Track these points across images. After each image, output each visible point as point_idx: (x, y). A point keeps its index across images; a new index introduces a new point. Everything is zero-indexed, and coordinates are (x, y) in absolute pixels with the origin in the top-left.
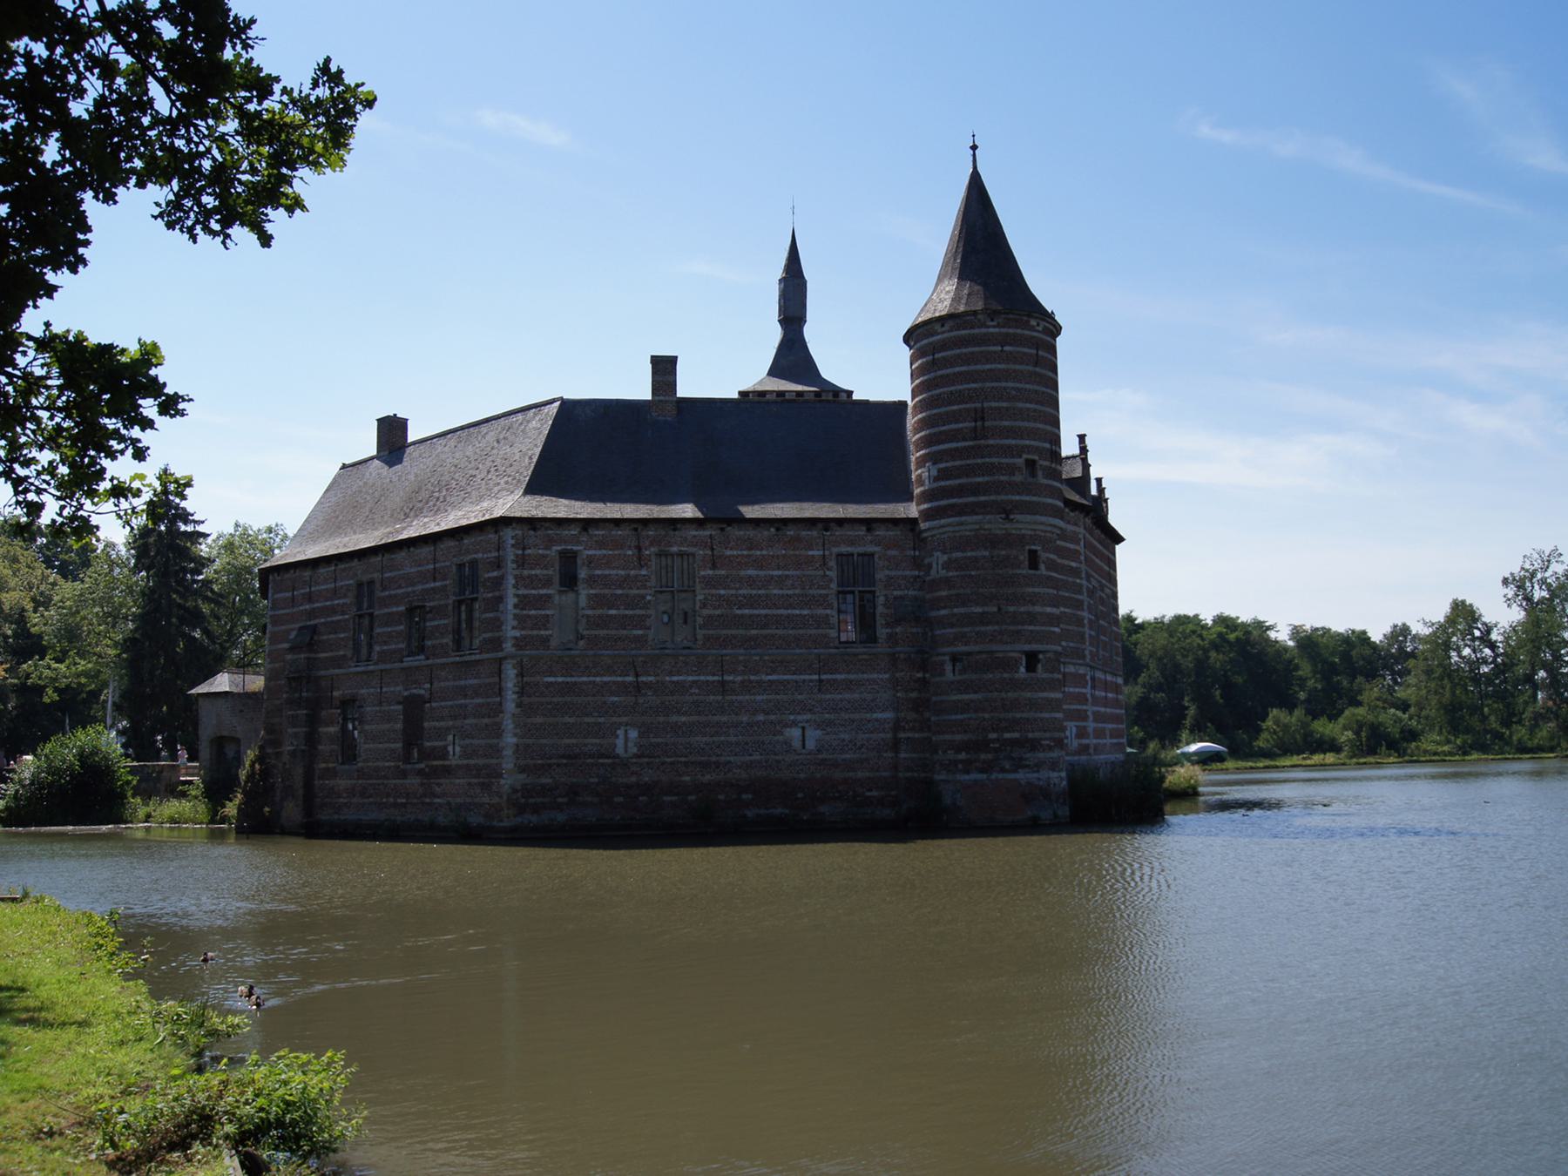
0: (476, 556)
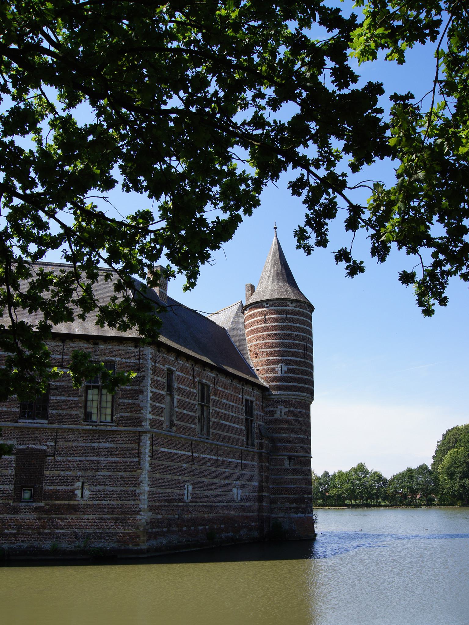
0: (114, 359)
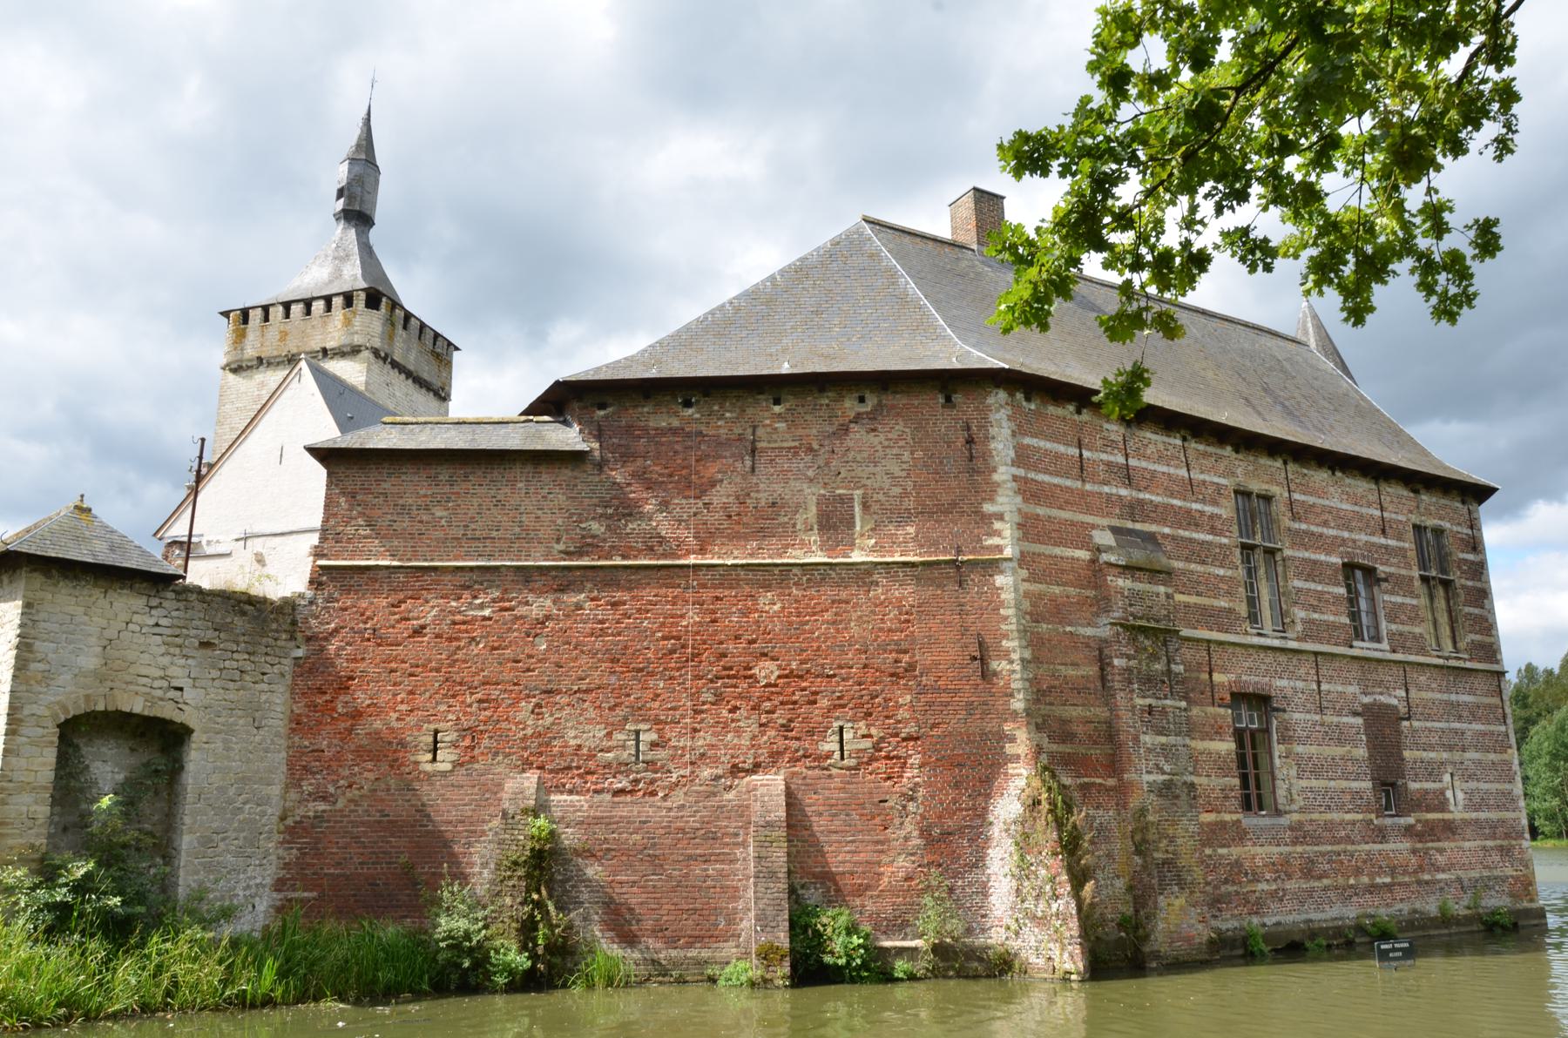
0: (1442, 523)
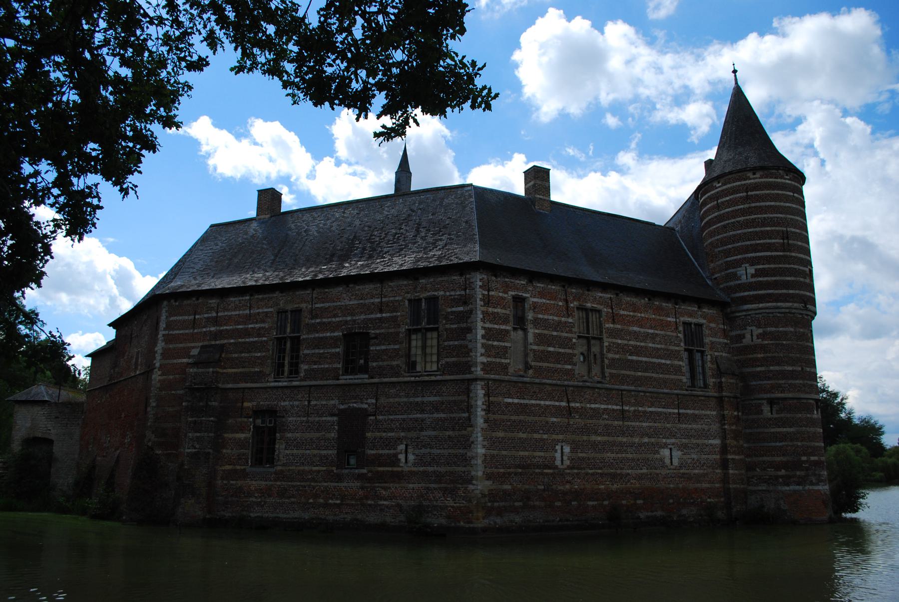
0: (436, 293)
